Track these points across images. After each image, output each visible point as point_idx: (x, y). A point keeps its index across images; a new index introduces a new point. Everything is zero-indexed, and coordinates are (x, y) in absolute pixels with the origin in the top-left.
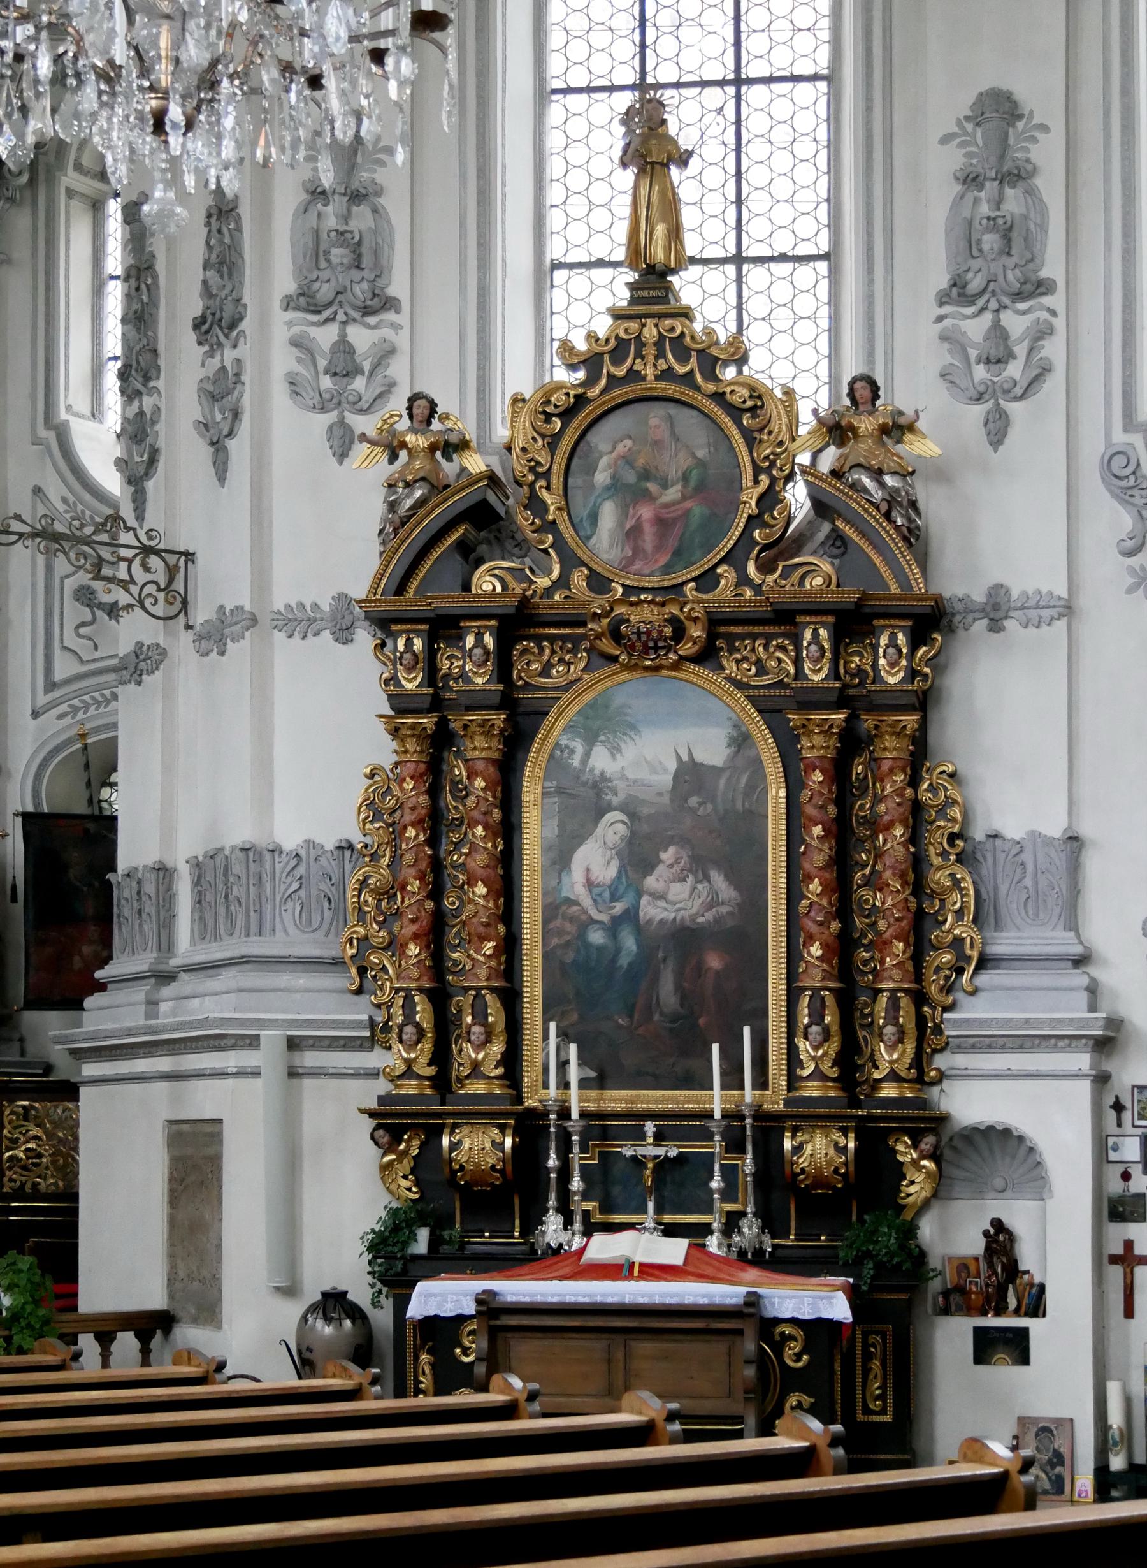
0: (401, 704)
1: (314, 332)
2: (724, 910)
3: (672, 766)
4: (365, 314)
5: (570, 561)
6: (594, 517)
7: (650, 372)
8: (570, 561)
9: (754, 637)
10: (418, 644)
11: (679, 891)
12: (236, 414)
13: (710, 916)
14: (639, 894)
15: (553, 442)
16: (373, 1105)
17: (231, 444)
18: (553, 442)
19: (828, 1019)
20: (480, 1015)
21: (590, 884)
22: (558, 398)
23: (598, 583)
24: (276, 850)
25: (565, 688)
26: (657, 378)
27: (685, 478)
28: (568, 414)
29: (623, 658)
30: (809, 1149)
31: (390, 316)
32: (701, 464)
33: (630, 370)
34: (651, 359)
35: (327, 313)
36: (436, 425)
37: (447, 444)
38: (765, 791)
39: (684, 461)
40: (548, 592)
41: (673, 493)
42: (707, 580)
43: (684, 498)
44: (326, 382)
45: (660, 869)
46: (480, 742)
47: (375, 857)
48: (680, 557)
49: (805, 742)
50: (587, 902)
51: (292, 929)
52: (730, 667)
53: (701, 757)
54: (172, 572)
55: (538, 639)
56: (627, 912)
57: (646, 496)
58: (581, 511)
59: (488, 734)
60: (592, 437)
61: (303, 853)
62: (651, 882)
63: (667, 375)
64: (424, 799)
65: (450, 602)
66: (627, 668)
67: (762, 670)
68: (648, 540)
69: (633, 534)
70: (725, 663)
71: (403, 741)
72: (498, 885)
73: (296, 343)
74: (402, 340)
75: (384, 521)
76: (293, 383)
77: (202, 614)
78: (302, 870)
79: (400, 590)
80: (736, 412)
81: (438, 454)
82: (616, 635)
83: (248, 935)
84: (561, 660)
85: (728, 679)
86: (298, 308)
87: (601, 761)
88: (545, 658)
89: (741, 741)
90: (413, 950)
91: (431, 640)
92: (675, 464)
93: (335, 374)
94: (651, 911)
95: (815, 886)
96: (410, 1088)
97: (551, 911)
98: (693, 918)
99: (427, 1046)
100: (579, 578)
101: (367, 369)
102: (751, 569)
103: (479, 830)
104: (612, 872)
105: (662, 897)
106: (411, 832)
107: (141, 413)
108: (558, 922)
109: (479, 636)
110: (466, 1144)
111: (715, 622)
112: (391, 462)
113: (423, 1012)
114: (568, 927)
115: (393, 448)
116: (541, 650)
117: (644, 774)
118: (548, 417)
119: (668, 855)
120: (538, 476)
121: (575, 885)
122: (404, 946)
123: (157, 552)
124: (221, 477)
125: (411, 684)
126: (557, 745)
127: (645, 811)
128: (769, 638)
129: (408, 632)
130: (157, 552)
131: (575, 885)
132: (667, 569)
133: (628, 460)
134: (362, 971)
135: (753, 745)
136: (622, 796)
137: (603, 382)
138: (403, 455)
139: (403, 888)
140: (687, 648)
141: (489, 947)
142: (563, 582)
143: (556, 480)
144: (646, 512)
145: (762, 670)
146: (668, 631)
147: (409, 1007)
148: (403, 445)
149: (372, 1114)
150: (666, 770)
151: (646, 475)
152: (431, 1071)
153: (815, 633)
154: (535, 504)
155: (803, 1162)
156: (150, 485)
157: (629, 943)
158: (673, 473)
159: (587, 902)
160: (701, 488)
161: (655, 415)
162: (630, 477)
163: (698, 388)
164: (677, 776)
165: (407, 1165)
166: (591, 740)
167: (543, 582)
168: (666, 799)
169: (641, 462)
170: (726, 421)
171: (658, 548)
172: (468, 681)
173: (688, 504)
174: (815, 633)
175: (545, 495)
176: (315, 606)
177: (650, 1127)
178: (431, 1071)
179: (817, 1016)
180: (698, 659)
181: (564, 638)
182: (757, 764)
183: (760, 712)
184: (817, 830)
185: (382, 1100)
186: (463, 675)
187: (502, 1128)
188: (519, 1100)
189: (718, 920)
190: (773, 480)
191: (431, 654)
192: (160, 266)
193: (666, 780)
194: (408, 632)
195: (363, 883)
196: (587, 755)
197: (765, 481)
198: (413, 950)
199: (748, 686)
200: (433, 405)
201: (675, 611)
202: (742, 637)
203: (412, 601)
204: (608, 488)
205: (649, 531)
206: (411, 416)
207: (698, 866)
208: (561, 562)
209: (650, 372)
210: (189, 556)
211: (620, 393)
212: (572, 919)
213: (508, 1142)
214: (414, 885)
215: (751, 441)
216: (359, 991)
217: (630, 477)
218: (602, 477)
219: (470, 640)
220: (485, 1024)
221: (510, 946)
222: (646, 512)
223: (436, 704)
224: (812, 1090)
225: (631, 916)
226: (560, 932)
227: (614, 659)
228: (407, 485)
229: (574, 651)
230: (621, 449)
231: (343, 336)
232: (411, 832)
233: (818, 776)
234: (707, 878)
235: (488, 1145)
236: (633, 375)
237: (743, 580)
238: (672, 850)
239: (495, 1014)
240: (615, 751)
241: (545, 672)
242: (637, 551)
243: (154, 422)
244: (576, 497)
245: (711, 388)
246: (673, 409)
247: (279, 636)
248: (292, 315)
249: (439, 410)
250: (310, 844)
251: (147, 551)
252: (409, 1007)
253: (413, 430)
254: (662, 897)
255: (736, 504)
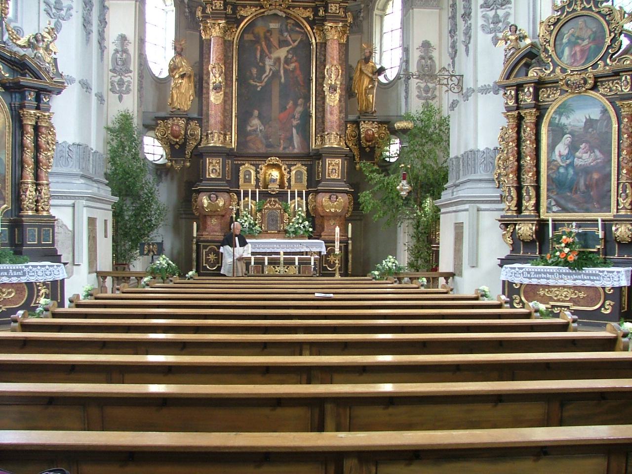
0: (508, 109)
1: (488, 13)
2: (599, 161)
3: (584, 120)
4: (502, 6)
5: (555, 65)
6: (563, 52)
7: (579, 9)
8: (555, 65)
9: (609, 81)
10: (513, 93)
11: (585, 156)
12: (470, 37)
13: (595, 163)
14: (574, 158)
15: (551, 32)
16: (499, 218)
17: (469, 45)
18: (551, 32)
19: (628, 192)
20: (528, 193)
21: (560, 155)
22: (552, 20)
23: (563, 70)
24: (478, 151)
25: (553, 101)
26: (581, 10)
27: (589, 38)
28: (555, 24)
29: (570, 91)
30: (620, 230)
31: (509, 5)
32: (595, 33)
33: (573, 9)
34: (579, 5)
35: (491, 8)
36: (518, 32)
37: (520, 37)
38: (612, 125)
39: (589, 32)
40: (549, 74)
41: (586, 42)
42: (595, 66)
43: (589, 43)
44: (492, 26)
45: (580, 150)
46: (529, 118)
47: (503, 151)
48: (587, 60)
49: (622, 110)
50: (559, 161)
51: (482, 172)
52: (601, 90)
53: (592, 117)
54: (459, 80)
55: (546, 88)
56: (570, 163)
57: (578, 44)
58: (559, 51)
59: (531, 116)
60: (562, 30)
61: (485, 151)
62: (577, 154)
63: (584, 9)
64: (515, 135)
65: (521, 79)
66: (571, 93)
67: (611, 90)
68: (578, 56)
69: (573, 56)
70: (600, 90)
71: (509, 119)
72: (534, 156)
73: (483, 16)
74: (512, 11)
75: (505, 60)
76: (483, 27)
77: (464, 91)
78: (485, 155)
79: (508, 78)
80: (604, 16)
81: (518, 41)
82: (568, 85)
83: (471, 174)
84: (553, 93)
85: (600, 94)
86: (484, 7)
87: (564, 120)
88: (548, 93)
89: (605, 111)
90: (511, 176)
91: (517, 91)
92: (587, 33)
93: (494, 23)
94: (577, 162)
95: (625, 152)
96: (510, 213)
97: (549, 163)
98: (590, 163)
99: (514, 202)
100: (558, 70)
101: (502, 21)
102: (608, 61)
103: (528, 142)
104: (566, 152)
105: (580, 158)
106: (511, 144)
107: (454, 41)
108: (551, 166)
109: (529, 88)
110: (522, 229)
111: (596, 78)
112: (506, 44)
113: (514, 193)
114: (554, 167)
115: (506, 40)
116: (547, 90)
117: (576, 124)
118: (550, 26)
119: (582, 146)
120: (547, 42)
121: (556, 156)
122: (509, 175)
123: (455, 76)
124: (467, 55)
125: (511, 103)
126: (551, 117)
127: (576, 134)
128: (613, 80)
129: (510, 89)
130: (455, 76)
131: (556, 156)
132: (583, 64)
133: (573, 35)
134: (499, 182)
135: (608, 113)
136: (569, 130)
137: (565, 13)
138: (509, 42)
139: (508, 159)
140: (588, 86)
141: (530, 174)
142: (553, 71)
143: (552, 43)
144: (578, 49)
145: (611, 90)
146: (582, 82)
147: (509, 191)
148: (509, 39)
149: (500, 221)
150: (582, 122)
151: (578, 38)
152: (516, 208)
153: (626, 78)
154: (546, 51)
155: (618, 233)
156: (456, 59)
157: (571, 171)
158: (586, 37)
159: (559, 161)
160: (594, 40)
161: (580, 21)
162: (573, 39)
163: (593, 11)
164: (585, 122)
165: (509, 234)
166: (561, 114)
167: (548, 72)
168: (582, 130)
169: (576, 35)
170: (601, 19)
171: (581, 59)
172: (526, 102)
173: (590, 45)
174: (626, 78)
175: (549, 48)
176: (489, 85)
177: (574, 224)
178: (516, 208)
179: (624, 191)
180: (592, 89)
181: (554, 87)
182: (609, 118)
183: (610, 102)
184: (626, 136)
185: (502, 217)
186: (525, 101)
187: (532, 224)
188: (539, 217)
189: (597, 163)
190: (616, 34)
191: (517, 95)
192: (457, 4)
193: (583, 124)
194: (510, 89)
195: (500, 158)
196: (560, 119)
197: (613, 35)
198: (511, 176)
199: (607, 95)
200: (516, 27)
201: (584, 76)
202: (605, 81)
203: (511, 81)
204: (566, 43)
205: (578, 54)
206: (510, 31)
207: (591, 149)
208: (553, 65)
209: (579, 9)
210: (463, 76)
211: (570, 16)
212: (555, 165)
213: (534, 228)
214: (511, 158)
215: (608, 24)
216: (498, 188)
217: (573, 39)
218: (565, 40)
219: (526, 90)
220: (529, 195)
221: (538, 173)
222: (578, 49)
223: (518, 108)
224: (622, 212)
225: (572, 164)
226: (552, 169)
227: (567, 91)
228: (510, 50)
229: (556, 90)
230: (571, 32)
231: (496, 13)
232: (511, 144)
233: (626, 120)
234: (594, 152)
235: (528, 229)
236: (574, 10)
237: (606, 65)
238: (584, 144)
239: (532, 193)
240: (568, 117)
241: (548, 97)
242: (575, 60)
243: (456, 43)
244: (558, 47)
245: (597, 10)
246: (585, 18)
247: (479, 94)
248: (482, 9)
249: (518, 28)
250: (487, 148)
251: (452, 76)
252: (509, 191)
253: (511, 35)
254: (580, 158)
255: (604, 43)
